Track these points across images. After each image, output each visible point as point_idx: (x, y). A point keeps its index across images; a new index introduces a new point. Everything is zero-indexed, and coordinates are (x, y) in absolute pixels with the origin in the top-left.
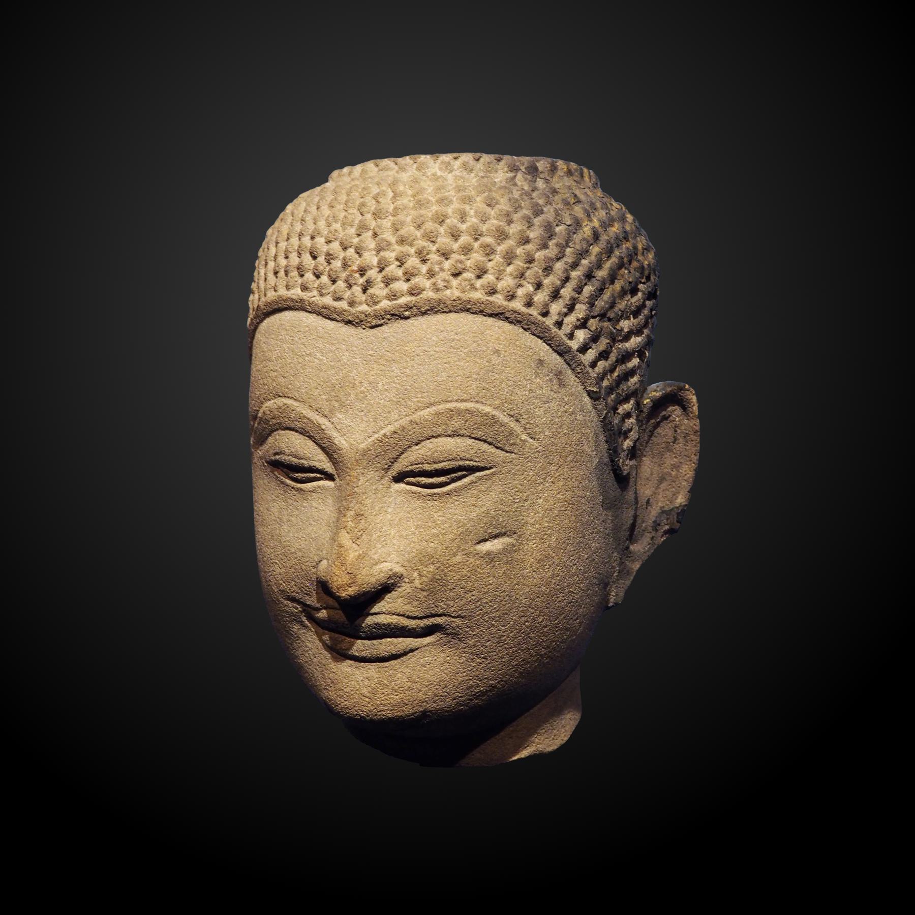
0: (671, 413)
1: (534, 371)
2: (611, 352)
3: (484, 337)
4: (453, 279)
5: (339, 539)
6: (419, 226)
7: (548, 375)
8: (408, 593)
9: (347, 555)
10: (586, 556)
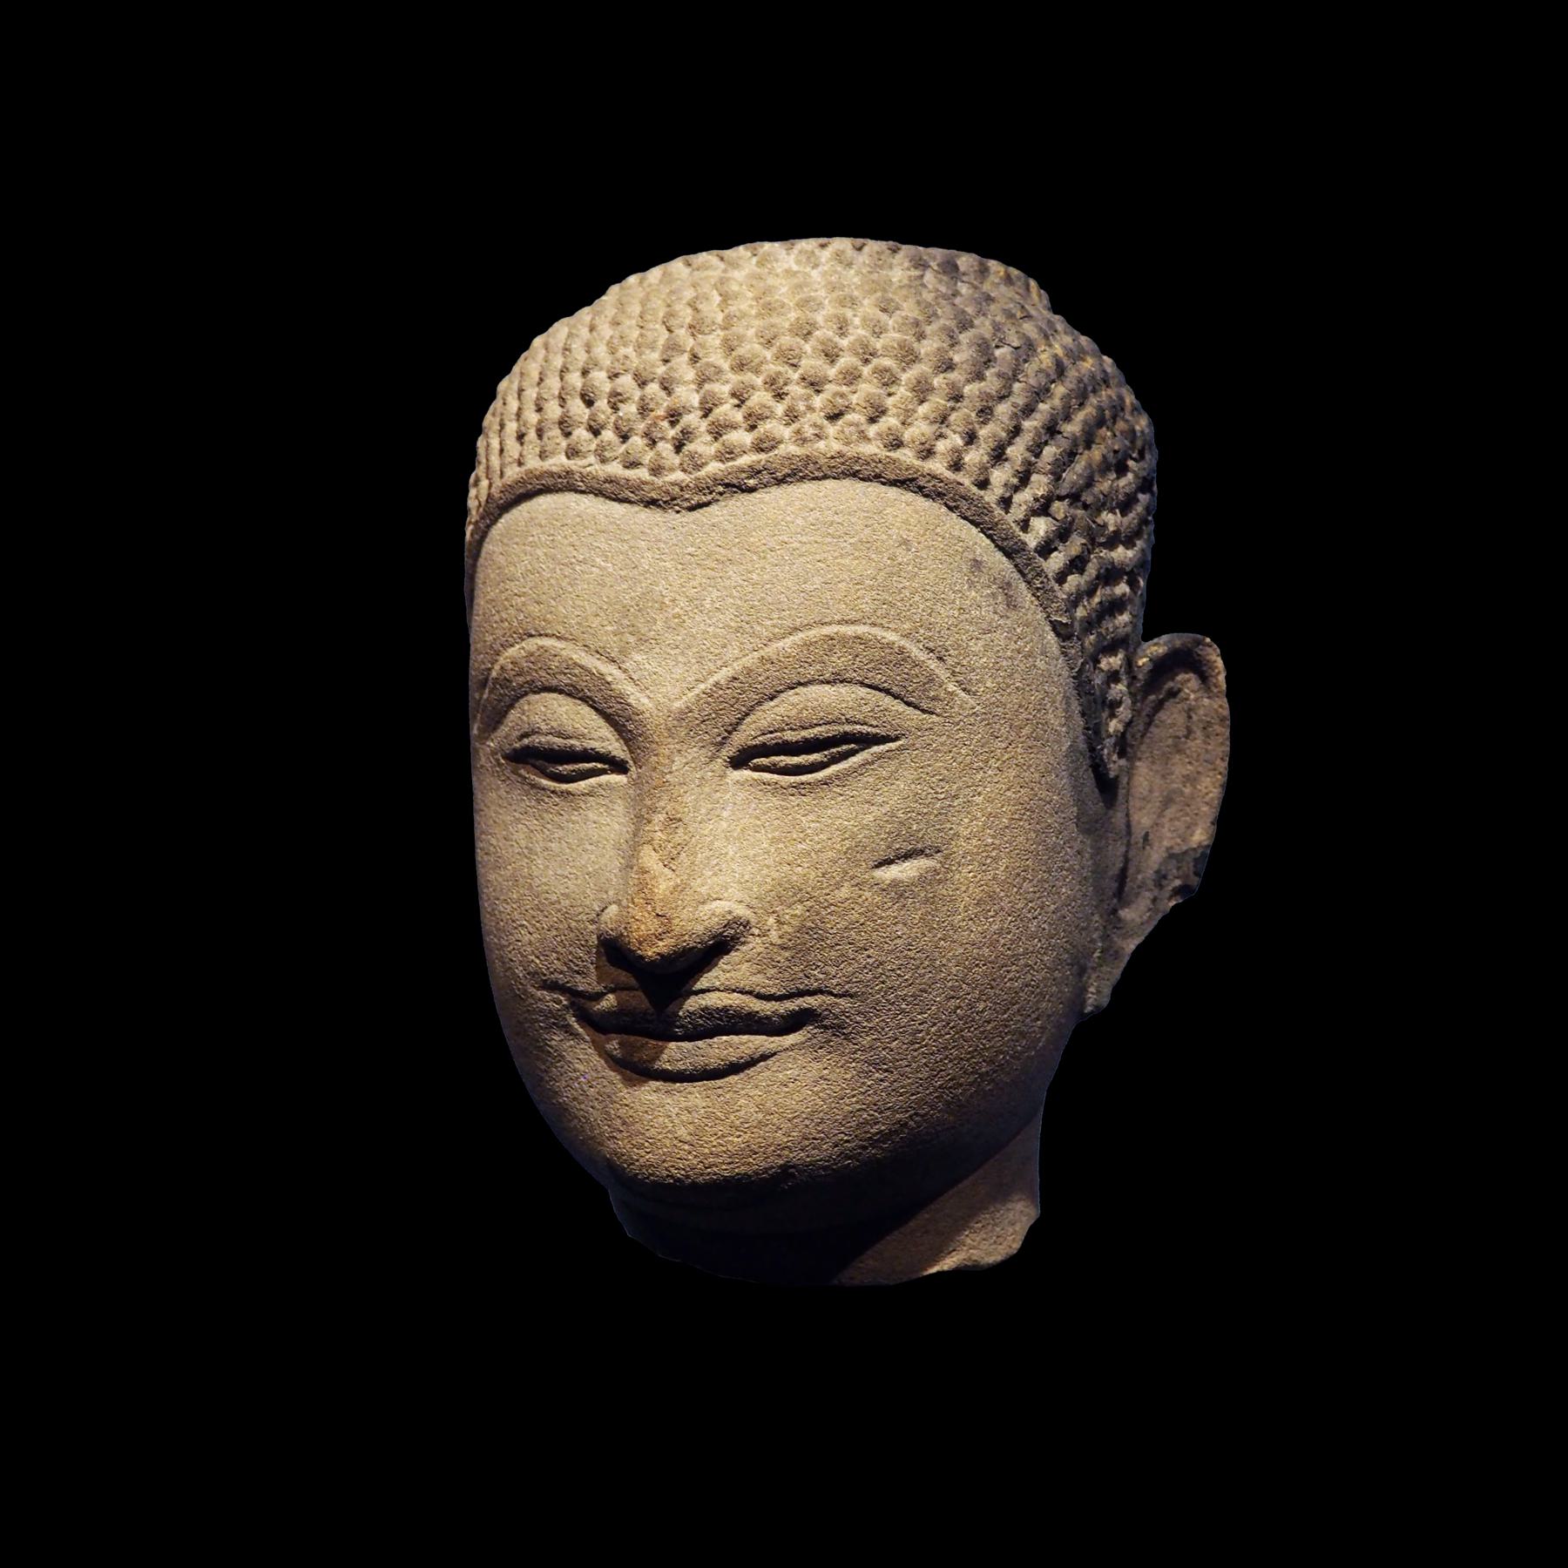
0: (1182, 684)
1: (966, 578)
2: (1089, 561)
3: (883, 518)
4: (829, 425)
5: (640, 861)
6: (770, 342)
7: (989, 587)
9: (656, 885)
10: (1053, 907)
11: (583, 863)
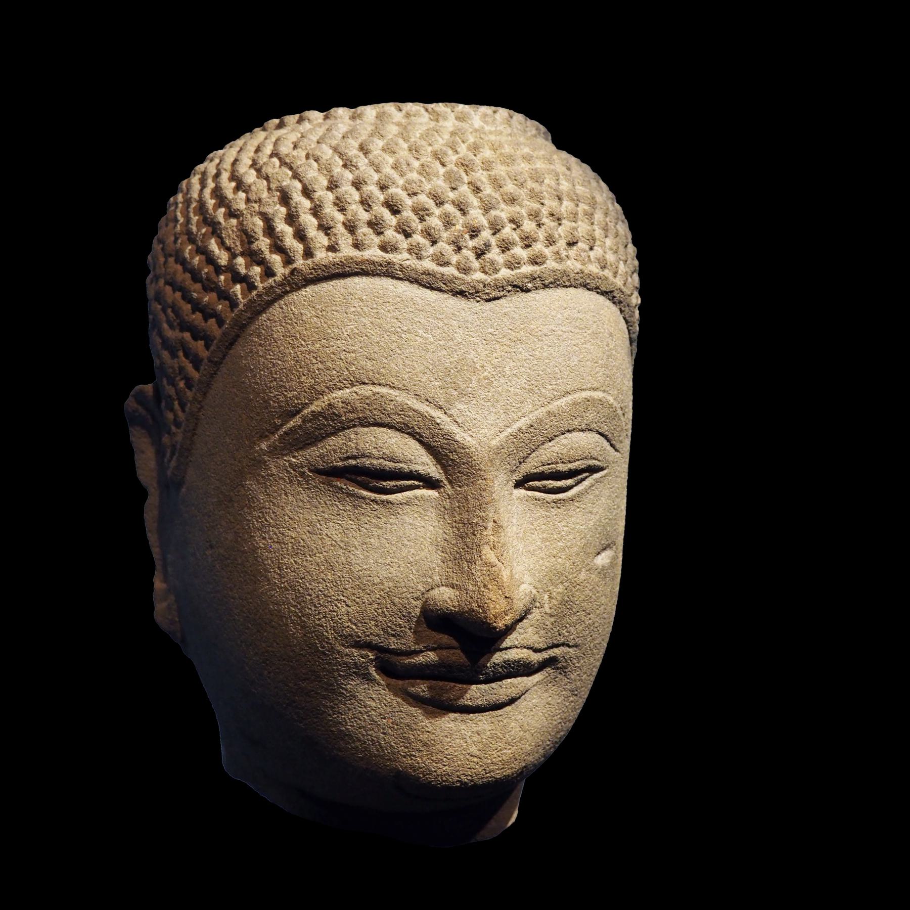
8: (538, 620)
11: (404, 555)
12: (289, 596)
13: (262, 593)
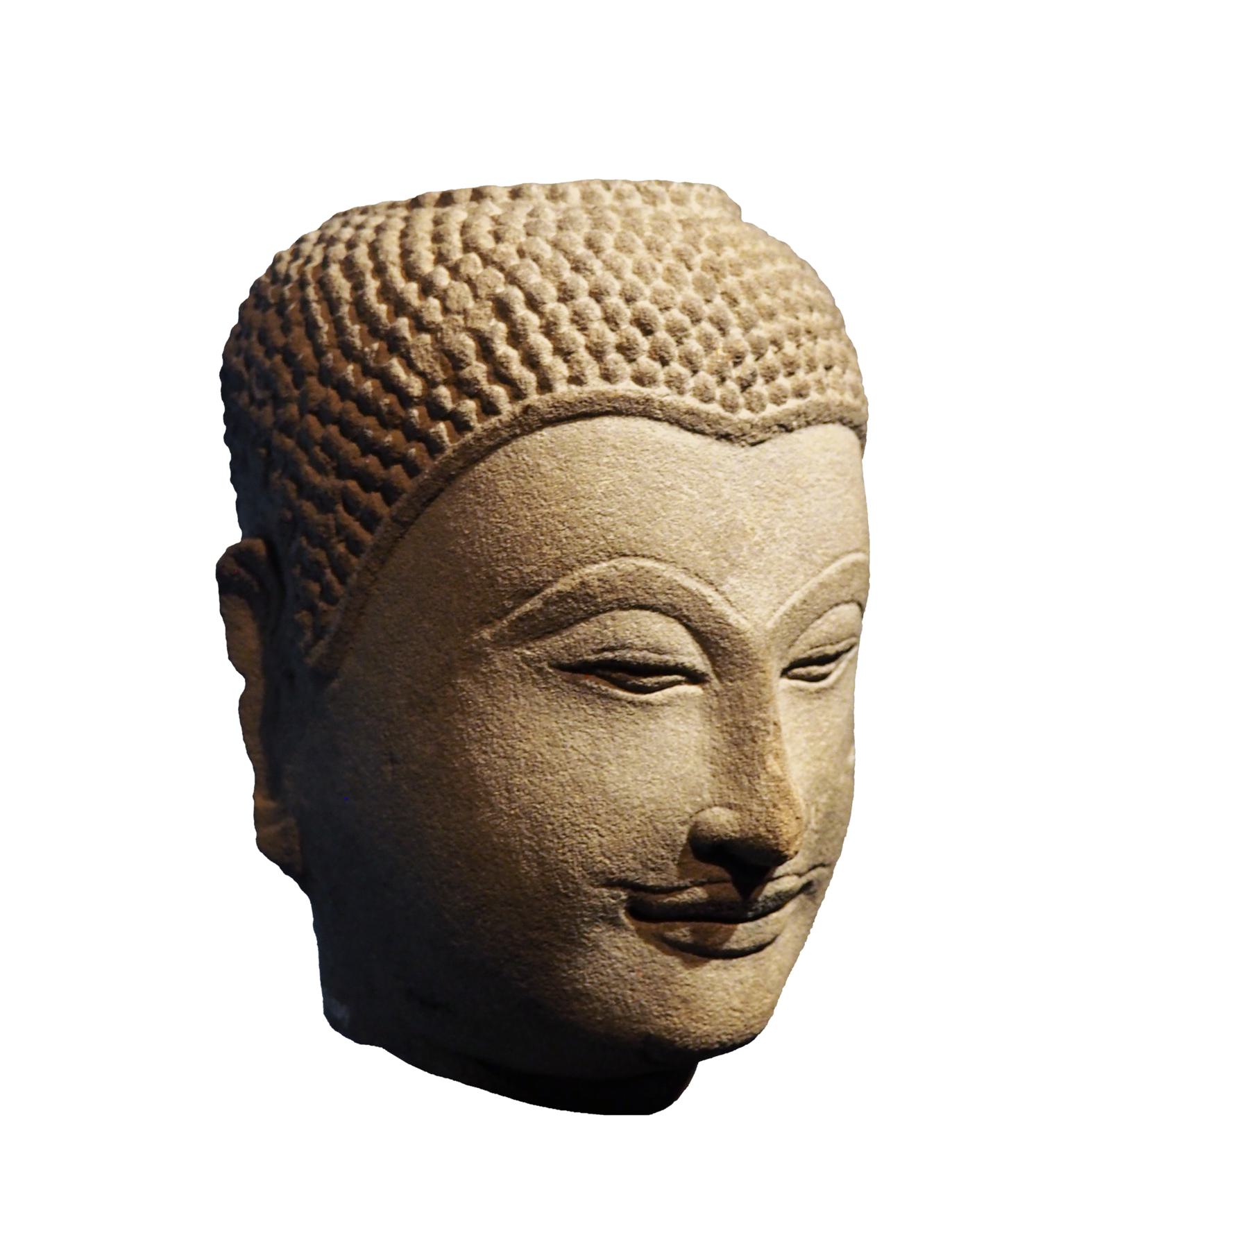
12: (522, 826)
13: (482, 821)
